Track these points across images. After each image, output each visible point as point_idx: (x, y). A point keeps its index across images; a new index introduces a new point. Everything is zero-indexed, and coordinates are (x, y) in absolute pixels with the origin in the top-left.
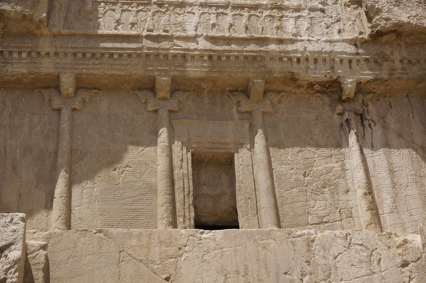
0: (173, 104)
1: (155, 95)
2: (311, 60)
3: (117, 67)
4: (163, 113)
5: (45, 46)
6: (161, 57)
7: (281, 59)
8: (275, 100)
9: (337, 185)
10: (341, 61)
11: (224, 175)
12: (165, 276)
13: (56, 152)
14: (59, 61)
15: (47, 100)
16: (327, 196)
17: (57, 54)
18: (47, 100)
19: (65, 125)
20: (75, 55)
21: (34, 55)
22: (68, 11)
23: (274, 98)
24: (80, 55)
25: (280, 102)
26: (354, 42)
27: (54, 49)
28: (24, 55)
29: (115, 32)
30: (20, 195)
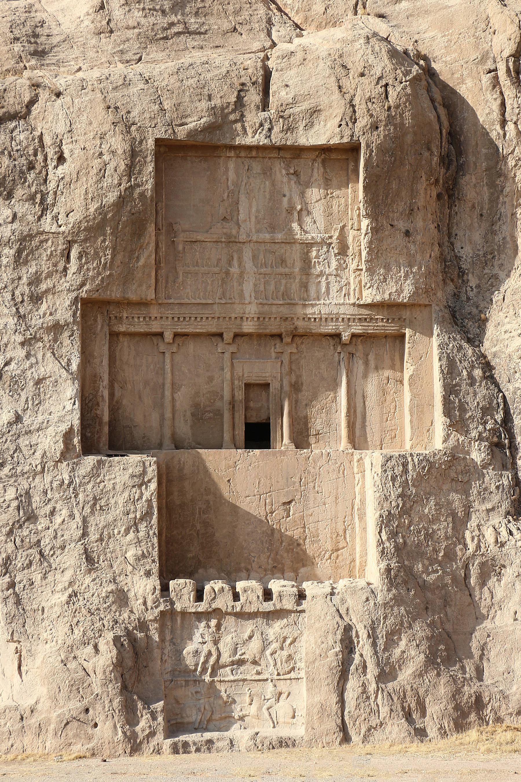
0: (233, 348)
1: (223, 340)
2: (323, 319)
3: (200, 327)
4: (227, 356)
5: (154, 312)
6: (227, 319)
7: (304, 318)
8: (300, 342)
9: (331, 408)
10: (343, 319)
11: (264, 393)
12: (227, 479)
13: (164, 385)
14: (163, 323)
15: (156, 344)
16: (323, 415)
17: (161, 318)
18: (156, 344)
19: (168, 367)
20: (173, 318)
21: (147, 319)
22: (167, 282)
23: (298, 340)
24: (176, 319)
25: (302, 343)
26: (354, 304)
27: (160, 315)
28: (141, 319)
29: (198, 301)
30: (145, 416)
